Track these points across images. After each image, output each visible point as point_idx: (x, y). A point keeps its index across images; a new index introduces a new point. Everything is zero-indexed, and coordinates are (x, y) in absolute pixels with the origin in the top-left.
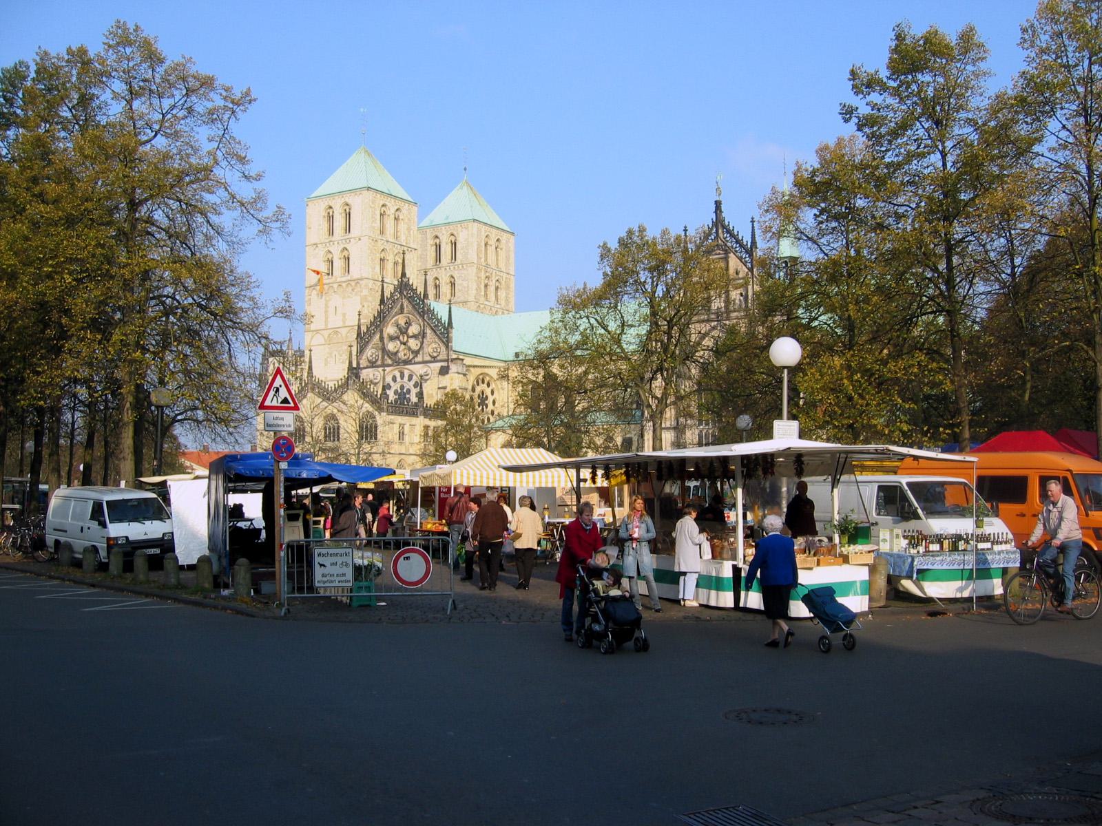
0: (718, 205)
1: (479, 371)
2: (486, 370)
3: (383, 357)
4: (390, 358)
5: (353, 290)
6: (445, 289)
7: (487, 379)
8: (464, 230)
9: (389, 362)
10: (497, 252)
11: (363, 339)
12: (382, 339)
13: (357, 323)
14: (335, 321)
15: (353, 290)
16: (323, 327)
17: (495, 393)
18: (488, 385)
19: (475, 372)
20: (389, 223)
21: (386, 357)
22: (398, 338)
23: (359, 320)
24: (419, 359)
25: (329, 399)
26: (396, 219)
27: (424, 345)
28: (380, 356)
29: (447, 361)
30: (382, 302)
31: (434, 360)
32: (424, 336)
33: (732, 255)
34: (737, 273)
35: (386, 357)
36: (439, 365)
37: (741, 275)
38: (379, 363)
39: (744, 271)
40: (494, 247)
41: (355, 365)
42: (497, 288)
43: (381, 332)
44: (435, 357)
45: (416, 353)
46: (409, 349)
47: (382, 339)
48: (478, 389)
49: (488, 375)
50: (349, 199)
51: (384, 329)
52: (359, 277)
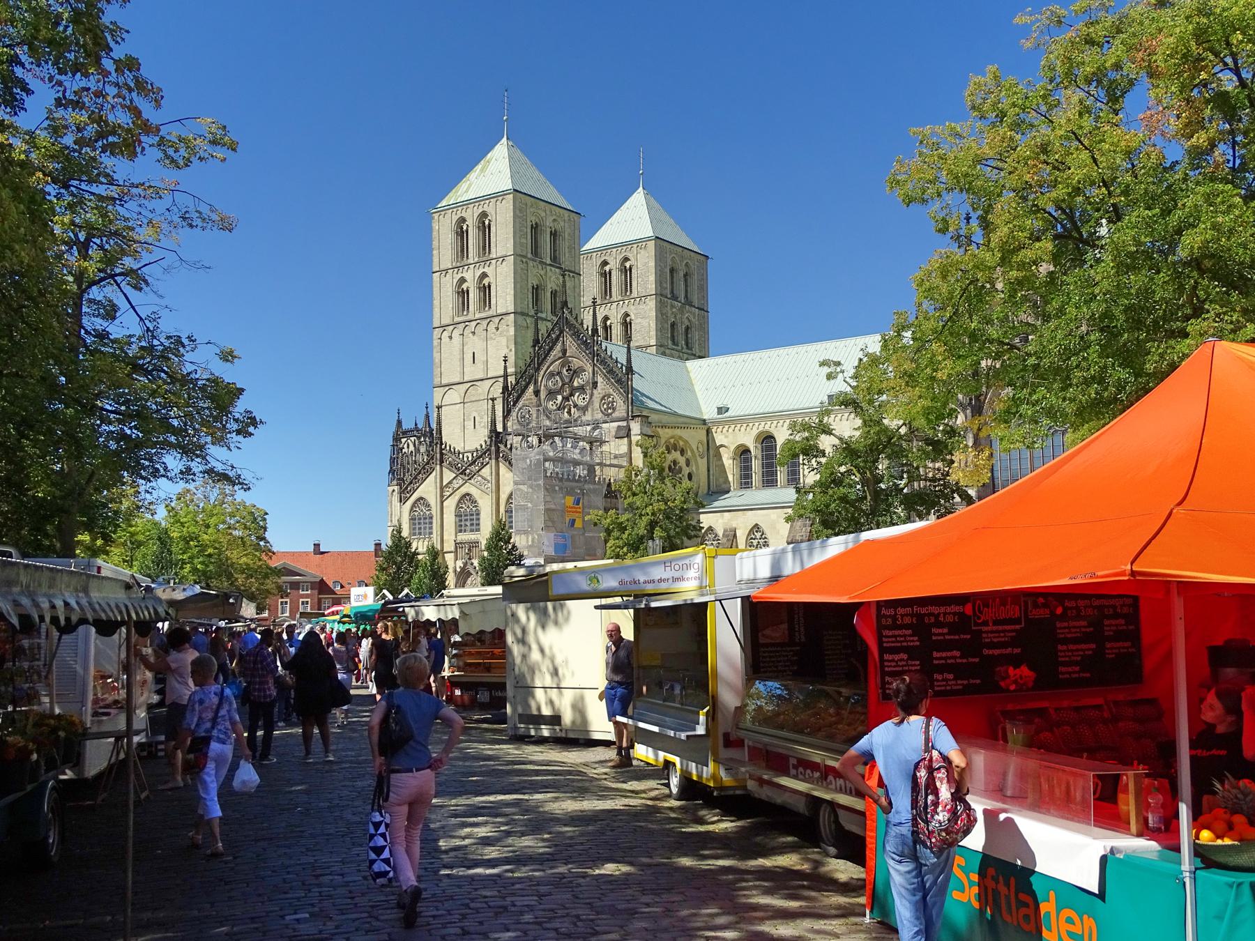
1: (669, 432)
2: (678, 432)
4: (548, 418)
5: (497, 329)
6: (617, 331)
7: (681, 443)
8: (642, 252)
10: (686, 281)
11: (511, 395)
12: (537, 393)
13: (502, 373)
14: (472, 372)
15: (497, 329)
16: (457, 380)
17: (692, 462)
18: (682, 452)
19: (665, 434)
20: (546, 240)
22: (559, 392)
23: (505, 368)
24: (588, 417)
25: (463, 473)
26: (554, 234)
29: (626, 419)
30: (536, 342)
31: (608, 418)
32: (595, 385)
36: (616, 424)
38: (533, 424)
40: (681, 274)
41: (500, 429)
42: (687, 329)
44: (608, 415)
45: (584, 409)
47: (537, 393)
48: (670, 457)
49: (680, 438)
50: (489, 208)
52: (504, 311)
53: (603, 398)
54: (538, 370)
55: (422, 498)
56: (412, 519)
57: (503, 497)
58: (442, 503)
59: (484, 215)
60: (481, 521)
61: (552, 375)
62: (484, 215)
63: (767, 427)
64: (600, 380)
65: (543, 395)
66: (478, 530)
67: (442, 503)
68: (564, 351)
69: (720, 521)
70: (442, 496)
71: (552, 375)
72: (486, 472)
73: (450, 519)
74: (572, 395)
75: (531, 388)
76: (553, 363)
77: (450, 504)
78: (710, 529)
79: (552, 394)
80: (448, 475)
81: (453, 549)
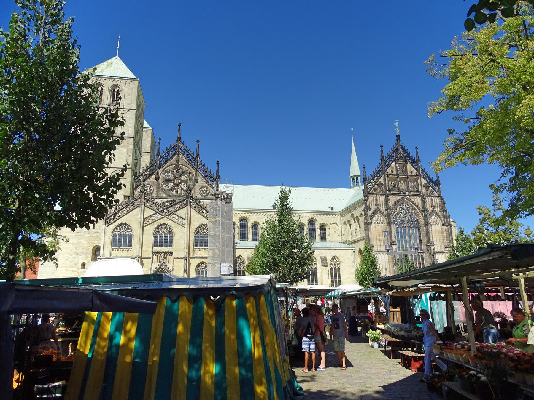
0: (398, 137)
3: (158, 192)
4: (165, 193)
9: (164, 195)
12: (157, 179)
21: (160, 192)
27: (196, 187)
28: (155, 191)
33: (408, 163)
34: (412, 172)
35: (160, 192)
37: (413, 174)
39: (415, 172)
43: (158, 173)
44: (204, 196)
46: (182, 189)
47: (157, 179)
50: (121, 84)
51: (160, 173)
53: (201, 188)
54: (160, 168)
55: (124, 224)
56: (114, 236)
57: (193, 228)
58: (143, 227)
59: (116, 86)
60: (174, 241)
61: (167, 172)
62: (116, 86)
63: (245, 215)
64: (200, 178)
65: (161, 181)
66: (172, 246)
67: (143, 227)
68: (178, 162)
69: (245, 253)
70: (143, 224)
71: (167, 172)
72: (183, 212)
73: (149, 238)
74: (180, 183)
75: (154, 176)
76: (170, 165)
77: (150, 230)
78: (239, 256)
79: (167, 181)
80: (149, 212)
81: (151, 256)
